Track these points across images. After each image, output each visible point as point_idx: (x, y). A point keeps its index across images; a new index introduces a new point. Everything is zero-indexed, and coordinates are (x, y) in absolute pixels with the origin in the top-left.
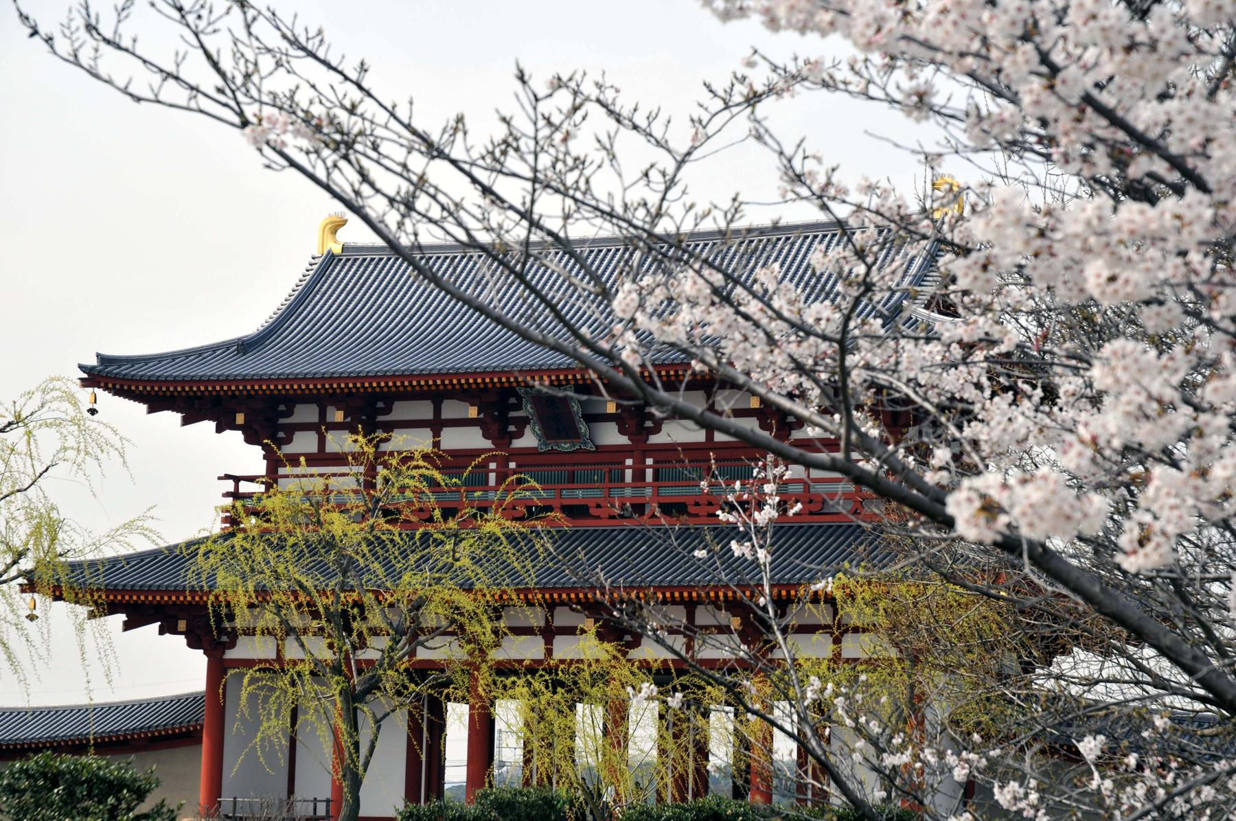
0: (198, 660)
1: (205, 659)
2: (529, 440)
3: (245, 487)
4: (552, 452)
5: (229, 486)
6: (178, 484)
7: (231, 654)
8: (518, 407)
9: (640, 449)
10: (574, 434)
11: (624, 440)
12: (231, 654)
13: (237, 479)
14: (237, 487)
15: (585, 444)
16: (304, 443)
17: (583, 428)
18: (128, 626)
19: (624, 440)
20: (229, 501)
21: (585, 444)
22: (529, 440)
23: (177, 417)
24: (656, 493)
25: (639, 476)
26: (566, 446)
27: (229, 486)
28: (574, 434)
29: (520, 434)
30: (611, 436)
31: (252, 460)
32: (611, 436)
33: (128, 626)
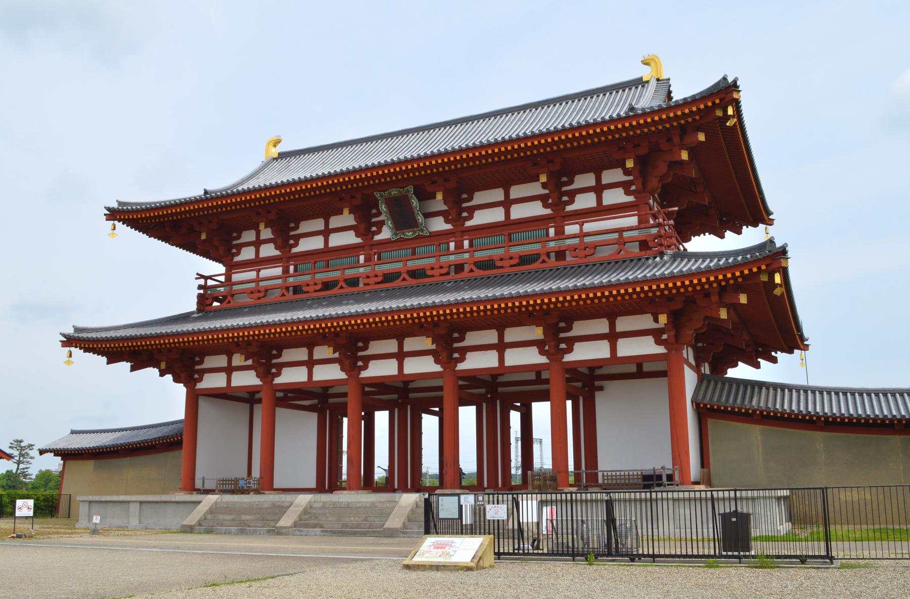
0: (180, 390)
1: (185, 389)
2: (386, 234)
3: (210, 283)
4: (401, 240)
5: (202, 282)
6: (168, 283)
7: (200, 386)
8: (379, 214)
11: (449, 227)
12: (200, 386)
13: (206, 278)
14: (206, 283)
15: (422, 231)
16: (247, 254)
17: (420, 218)
20: (202, 291)
21: (422, 231)
22: (386, 234)
24: (472, 256)
25: (459, 246)
26: (409, 234)
27: (202, 282)
28: (412, 224)
29: (379, 232)
30: (439, 225)
32: (439, 225)
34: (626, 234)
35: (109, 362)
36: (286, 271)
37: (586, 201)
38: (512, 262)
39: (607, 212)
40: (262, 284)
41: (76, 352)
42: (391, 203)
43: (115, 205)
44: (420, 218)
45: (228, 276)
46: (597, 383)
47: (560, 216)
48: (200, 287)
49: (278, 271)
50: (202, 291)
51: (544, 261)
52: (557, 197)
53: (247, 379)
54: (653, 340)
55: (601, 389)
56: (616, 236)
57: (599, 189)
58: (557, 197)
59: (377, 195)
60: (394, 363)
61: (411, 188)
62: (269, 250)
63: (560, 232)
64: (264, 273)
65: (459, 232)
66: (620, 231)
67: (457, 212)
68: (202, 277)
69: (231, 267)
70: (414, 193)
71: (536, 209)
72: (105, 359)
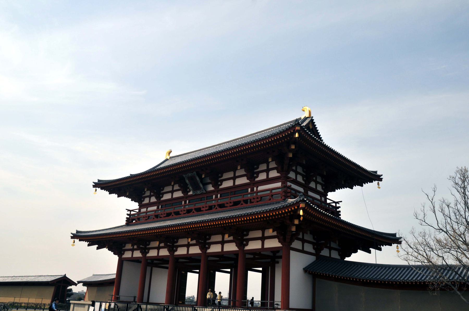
0: (116, 258)
1: (118, 258)
3: (132, 213)
5: (129, 213)
9: (217, 190)
10: (199, 188)
11: (213, 189)
13: (131, 211)
16: (146, 201)
18: (98, 248)
19: (213, 189)
20: (128, 217)
23: (108, 193)
27: (129, 213)
28: (199, 188)
29: (190, 191)
31: (135, 206)
33: (98, 248)
34: (273, 191)
35: (89, 245)
36: (158, 208)
37: (262, 176)
38: (231, 204)
39: (269, 181)
40: (148, 213)
41: (77, 241)
42: (192, 179)
43: (97, 181)
44: (201, 186)
45: (139, 210)
46: (276, 260)
47: (254, 183)
48: (128, 214)
49: (155, 208)
50: (128, 217)
51: (242, 204)
52: (252, 175)
53: (137, 254)
54: (278, 240)
55: (278, 262)
56: (269, 192)
57: (267, 171)
58: (252, 175)
59: (184, 176)
60: (185, 249)
61: (195, 173)
62: (153, 199)
63: (252, 190)
64: (149, 209)
65: (217, 190)
66: (271, 190)
67: (217, 182)
68: (129, 210)
69: (141, 206)
70: (197, 175)
71: (244, 180)
72: (87, 243)
